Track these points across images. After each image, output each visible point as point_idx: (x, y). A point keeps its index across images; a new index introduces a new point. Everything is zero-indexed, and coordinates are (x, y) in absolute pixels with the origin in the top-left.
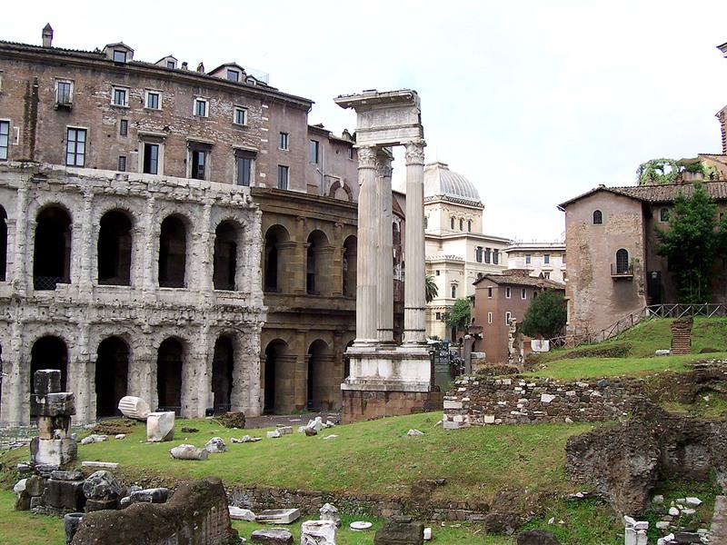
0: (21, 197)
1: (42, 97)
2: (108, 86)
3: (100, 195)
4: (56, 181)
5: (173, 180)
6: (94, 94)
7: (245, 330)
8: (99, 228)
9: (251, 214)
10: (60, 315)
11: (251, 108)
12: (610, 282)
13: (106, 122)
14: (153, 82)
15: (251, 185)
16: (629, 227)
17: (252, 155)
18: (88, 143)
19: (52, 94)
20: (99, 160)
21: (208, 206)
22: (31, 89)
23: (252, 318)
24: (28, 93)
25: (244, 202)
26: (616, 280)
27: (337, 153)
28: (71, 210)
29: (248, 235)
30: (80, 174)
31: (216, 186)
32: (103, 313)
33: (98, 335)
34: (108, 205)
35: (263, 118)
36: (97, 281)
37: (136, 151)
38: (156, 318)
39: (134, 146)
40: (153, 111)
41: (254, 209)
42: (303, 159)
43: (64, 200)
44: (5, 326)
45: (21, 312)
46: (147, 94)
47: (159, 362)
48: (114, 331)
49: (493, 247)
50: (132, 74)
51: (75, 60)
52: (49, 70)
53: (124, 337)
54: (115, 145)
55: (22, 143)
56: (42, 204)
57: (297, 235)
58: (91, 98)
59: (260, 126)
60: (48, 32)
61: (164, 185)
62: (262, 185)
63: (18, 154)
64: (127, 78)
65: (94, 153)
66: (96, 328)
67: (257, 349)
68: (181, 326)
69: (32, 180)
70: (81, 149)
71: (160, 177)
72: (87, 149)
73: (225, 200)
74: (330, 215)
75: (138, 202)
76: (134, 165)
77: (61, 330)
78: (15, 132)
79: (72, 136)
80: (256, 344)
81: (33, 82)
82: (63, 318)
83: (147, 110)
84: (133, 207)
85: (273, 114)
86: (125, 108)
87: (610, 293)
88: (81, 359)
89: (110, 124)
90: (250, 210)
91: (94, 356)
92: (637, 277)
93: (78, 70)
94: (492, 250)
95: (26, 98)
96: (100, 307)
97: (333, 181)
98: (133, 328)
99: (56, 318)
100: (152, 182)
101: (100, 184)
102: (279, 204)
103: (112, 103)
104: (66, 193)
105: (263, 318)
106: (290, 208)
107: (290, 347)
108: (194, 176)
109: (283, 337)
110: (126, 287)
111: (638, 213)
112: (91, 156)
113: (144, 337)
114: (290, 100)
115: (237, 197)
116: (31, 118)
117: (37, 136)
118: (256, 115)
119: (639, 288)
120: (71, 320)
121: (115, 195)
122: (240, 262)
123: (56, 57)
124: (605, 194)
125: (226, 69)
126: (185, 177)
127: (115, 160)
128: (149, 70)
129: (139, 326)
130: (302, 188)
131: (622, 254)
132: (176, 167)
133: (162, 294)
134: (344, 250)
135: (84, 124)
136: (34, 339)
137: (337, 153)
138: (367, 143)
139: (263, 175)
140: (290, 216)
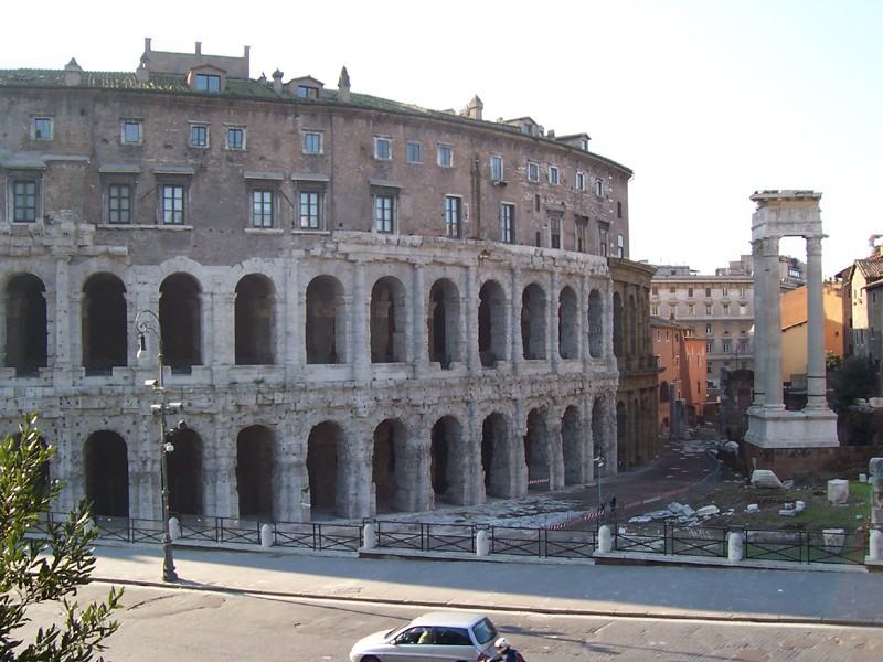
1: (482, 174)
2: (525, 161)
19: (489, 168)
21: (587, 278)
30: (513, 250)
60: (198, 46)
83: (551, 186)
95: (472, 173)
108: (554, 247)
120: (514, 396)
127: (533, 237)
135: (513, 200)
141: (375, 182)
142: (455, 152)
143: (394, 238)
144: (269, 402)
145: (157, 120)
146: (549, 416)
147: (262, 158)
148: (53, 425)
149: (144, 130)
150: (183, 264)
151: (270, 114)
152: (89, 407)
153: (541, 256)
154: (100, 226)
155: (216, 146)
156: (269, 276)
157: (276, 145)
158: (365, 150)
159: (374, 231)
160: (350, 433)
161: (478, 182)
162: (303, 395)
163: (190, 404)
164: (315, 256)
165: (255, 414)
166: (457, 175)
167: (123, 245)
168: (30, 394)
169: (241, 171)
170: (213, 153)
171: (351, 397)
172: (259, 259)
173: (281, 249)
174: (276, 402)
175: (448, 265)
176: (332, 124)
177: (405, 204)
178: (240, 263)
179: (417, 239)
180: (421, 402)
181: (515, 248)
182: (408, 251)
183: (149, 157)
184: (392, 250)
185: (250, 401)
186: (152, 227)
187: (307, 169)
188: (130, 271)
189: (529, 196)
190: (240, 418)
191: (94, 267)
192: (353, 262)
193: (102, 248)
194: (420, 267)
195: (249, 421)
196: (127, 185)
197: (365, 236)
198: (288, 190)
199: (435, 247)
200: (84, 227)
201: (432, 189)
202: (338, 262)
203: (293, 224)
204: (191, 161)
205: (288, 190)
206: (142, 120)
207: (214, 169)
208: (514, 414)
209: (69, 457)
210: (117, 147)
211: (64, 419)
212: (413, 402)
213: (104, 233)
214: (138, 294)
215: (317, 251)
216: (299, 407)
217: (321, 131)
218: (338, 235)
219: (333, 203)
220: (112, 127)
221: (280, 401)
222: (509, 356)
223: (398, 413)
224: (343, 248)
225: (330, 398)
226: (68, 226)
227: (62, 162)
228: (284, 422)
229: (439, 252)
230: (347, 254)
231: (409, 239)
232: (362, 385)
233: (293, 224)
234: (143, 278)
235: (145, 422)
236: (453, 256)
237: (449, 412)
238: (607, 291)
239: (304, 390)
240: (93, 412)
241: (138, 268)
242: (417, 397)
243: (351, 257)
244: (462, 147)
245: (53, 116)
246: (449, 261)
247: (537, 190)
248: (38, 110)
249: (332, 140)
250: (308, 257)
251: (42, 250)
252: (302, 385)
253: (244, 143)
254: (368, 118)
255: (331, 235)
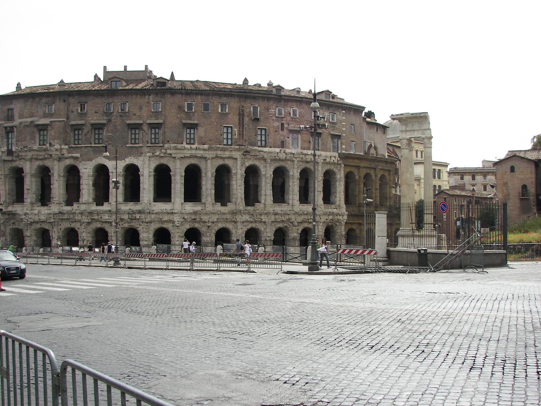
0: (239, 162)
1: (246, 114)
2: (274, 107)
3: (274, 160)
4: (254, 154)
5: (305, 152)
6: (269, 111)
7: (337, 224)
8: (272, 176)
9: (339, 166)
10: (258, 218)
11: (338, 113)
12: (518, 201)
13: (275, 125)
14: (294, 104)
15: (339, 152)
16: (528, 174)
17: (339, 137)
18: (267, 135)
20: (272, 143)
22: (241, 111)
23: (341, 218)
24: (239, 112)
25: (336, 161)
26: (521, 199)
27: (370, 129)
28: (260, 168)
29: (338, 176)
31: (323, 153)
32: (277, 217)
33: (274, 227)
34: (277, 165)
35: (343, 118)
36: (272, 202)
37: (288, 138)
38: (300, 219)
39: (287, 135)
40: (295, 118)
41: (340, 164)
42: (361, 137)
43: (257, 163)
44: (234, 224)
45: (241, 217)
46: (292, 110)
47: (300, 240)
48: (281, 225)
49: (437, 168)
50: (285, 100)
51: (260, 95)
52: (248, 101)
53: (284, 228)
54: (279, 136)
55: (238, 137)
56: (248, 166)
57: (359, 175)
58: (267, 113)
59: (342, 122)
61: (301, 154)
62: (343, 152)
63: (237, 142)
64: (282, 102)
65: (270, 140)
66: (273, 224)
67: (344, 233)
68: (310, 223)
69: (243, 154)
70: (263, 138)
71: (299, 150)
72: (267, 138)
73: (328, 160)
74: (373, 165)
75: (289, 163)
76: (288, 145)
77: (257, 225)
78: (235, 132)
79: (259, 132)
80: (343, 230)
81: (241, 107)
82: (260, 220)
83: (292, 118)
84: (288, 165)
85: (347, 115)
86: (283, 117)
87: (518, 205)
88: (268, 239)
89: (276, 125)
90: (338, 164)
91: (273, 238)
92: (532, 198)
93: (261, 100)
94: (437, 170)
95: (239, 115)
96: (276, 214)
97: (369, 144)
98: (289, 224)
99: (256, 219)
100: (296, 153)
101: (273, 155)
102: (351, 160)
103: (277, 115)
104: (258, 160)
105: (346, 217)
106: (356, 162)
107: (358, 231)
109: (354, 227)
110: (286, 204)
111: (533, 168)
112: (269, 142)
113: (294, 228)
114: (355, 108)
115: (333, 158)
116: (241, 124)
117: (244, 133)
118: (340, 116)
119: (533, 204)
121: (280, 160)
122: (333, 190)
123: (252, 94)
124: (515, 158)
125: (324, 93)
126: (310, 150)
127: (279, 143)
128: (293, 98)
129: (292, 223)
130: (361, 152)
131: (524, 187)
132: (306, 145)
133: (301, 207)
134: (380, 182)
135: (265, 126)
136: (246, 230)
137: (370, 129)
138: (405, 137)
139: (344, 147)
140: (355, 166)
141: (184, 121)
142: (229, 105)
143: (194, 146)
144: (134, 218)
145: (92, 102)
146: (290, 232)
147: (135, 115)
148: (52, 225)
149: (87, 106)
150: (101, 160)
151: (138, 96)
152: (64, 218)
153: (284, 152)
154: (70, 146)
155: (116, 111)
156: (136, 165)
157: (141, 108)
158: (180, 108)
159: (185, 143)
160: (172, 233)
161: (243, 119)
162: (149, 216)
163: (101, 218)
164: (157, 156)
165: (128, 223)
166: (230, 116)
167: (78, 153)
168: (43, 213)
169: (125, 120)
170: (114, 114)
171: (171, 217)
172: (133, 157)
173: (142, 153)
174: (137, 218)
175: (225, 158)
176: (165, 98)
177: (201, 131)
178: (125, 159)
179: (206, 146)
180: (207, 221)
181: (266, 149)
182: (202, 152)
183: (89, 117)
184: (194, 152)
185: (126, 217)
186: (89, 145)
187: (154, 118)
188: (81, 164)
189: (277, 124)
190: (122, 225)
191: (68, 162)
192: (175, 158)
193: (70, 155)
194: (208, 159)
195: (126, 225)
196: (158, 128)
197: (179, 146)
198: (145, 128)
199: (216, 150)
200: (63, 147)
201: (215, 123)
202: (168, 158)
203: (147, 142)
204: (105, 118)
205: (145, 128)
206: (86, 102)
207: (114, 121)
208: (265, 229)
209: (56, 238)
210: (77, 114)
211: (55, 222)
212: (203, 220)
213: (72, 149)
214: (83, 173)
215: (157, 153)
216: (147, 220)
217: (160, 101)
218: (166, 146)
219: (165, 132)
220: (75, 106)
221: (139, 218)
222: (263, 201)
223: (197, 225)
224: (169, 152)
225: (161, 217)
226: (57, 146)
227: (56, 121)
228: (141, 227)
229: (219, 152)
230: (171, 154)
231: (201, 146)
232: (176, 211)
233: (147, 142)
234: (85, 167)
235: (84, 225)
236: (227, 154)
237: (224, 226)
238: (340, 170)
239: (149, 213)
240: (66, 220)
241: (83, 162)
242: (205, 218)
243: (173, 156)
244: (234, 104)
245: (54, 103)
246: (224, 156)
247: (282, 120)
248: (49, 101)
249: (165, 104)
250: (154, 156)
251: (49, 157)
252: (148, 211)
253: (127, 109)
254: (182, 94)
255: (164, 146)
